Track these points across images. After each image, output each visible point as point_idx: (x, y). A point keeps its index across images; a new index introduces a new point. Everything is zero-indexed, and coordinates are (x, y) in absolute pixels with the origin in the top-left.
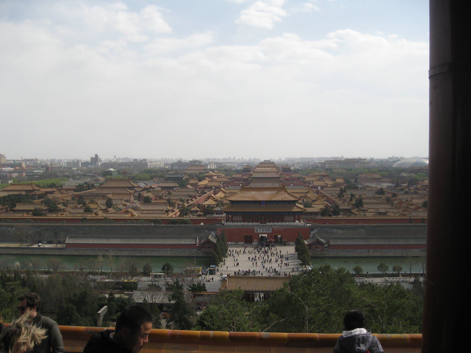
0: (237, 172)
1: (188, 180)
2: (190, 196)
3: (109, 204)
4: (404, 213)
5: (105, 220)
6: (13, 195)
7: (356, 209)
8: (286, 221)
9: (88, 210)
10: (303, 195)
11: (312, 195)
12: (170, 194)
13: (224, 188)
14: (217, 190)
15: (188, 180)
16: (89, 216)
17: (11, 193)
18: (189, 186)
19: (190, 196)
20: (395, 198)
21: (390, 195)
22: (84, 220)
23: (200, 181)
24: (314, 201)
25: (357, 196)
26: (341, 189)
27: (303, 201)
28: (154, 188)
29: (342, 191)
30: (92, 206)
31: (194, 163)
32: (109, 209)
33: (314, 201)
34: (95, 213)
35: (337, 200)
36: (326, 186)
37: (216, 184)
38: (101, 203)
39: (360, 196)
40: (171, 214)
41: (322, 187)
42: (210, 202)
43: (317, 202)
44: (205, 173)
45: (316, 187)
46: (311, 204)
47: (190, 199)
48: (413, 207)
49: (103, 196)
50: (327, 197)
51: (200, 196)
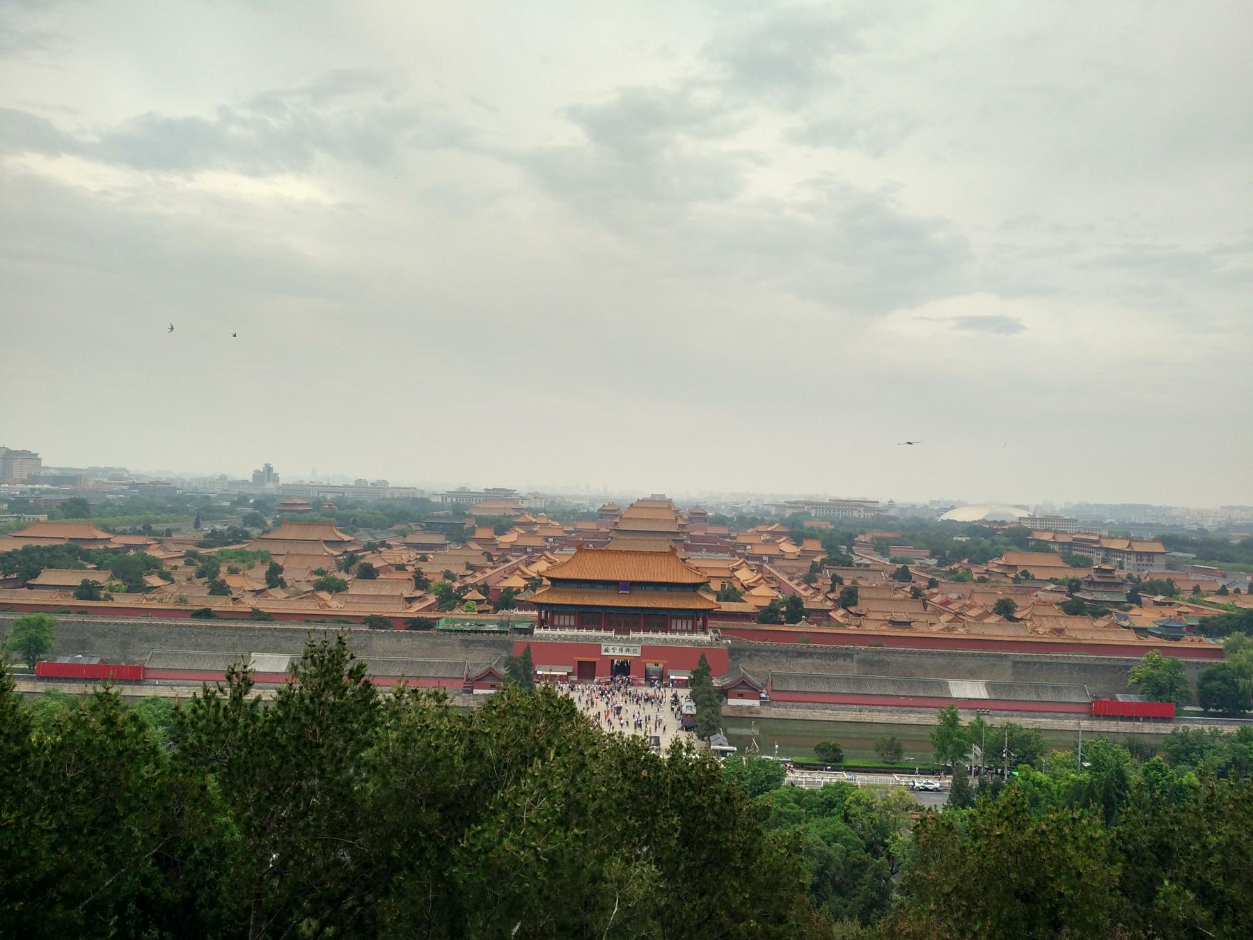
0: (589, 516)
1: (473, 529)
2: (469, 567)
3: (274, 578)
4: (953, 625)
5: (257, 615)
6: (38, 547)
7: (841, 612)
8: (674, 631)
9: (219, 589)
10: (728, 574)
11: (745, 576)
12: (424, 559)
13: (552, 553)
14: (533, 554)
15: (473, 529)
16: (218, 604)
17: (34, 543)
18: (474, 546)
19: (469, 567)
20: (935, 590)
21: (924, 584)
22: (206, 614)
23: (503, 534)
24: (749, 588)
25: (847, 583)
26: (814, 565)
27: (723, 586)
28: (389, 547)
29: (816, 569)
30: (233, 582)
31: (493, 495)
32: (270, 591)
33: (749, 588)
34: (235, 599)
35: (800, 589)
36: (782, 556)
37: (538, 542)
38: (256, 577)
39: (854, 582)
40: (417, 606)
41: (772, 559)
42: (516, 582)
43: (753, 592)
44: (516, 516)
45: (759, 558)
46: (741, 594)
47: (469, 572)
48: (973, 613)
49: (265, 557)
50: (781, 582)
51: (493, 568)
